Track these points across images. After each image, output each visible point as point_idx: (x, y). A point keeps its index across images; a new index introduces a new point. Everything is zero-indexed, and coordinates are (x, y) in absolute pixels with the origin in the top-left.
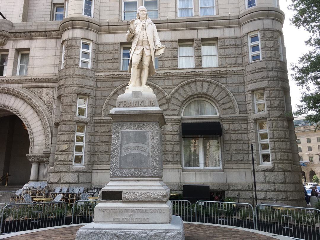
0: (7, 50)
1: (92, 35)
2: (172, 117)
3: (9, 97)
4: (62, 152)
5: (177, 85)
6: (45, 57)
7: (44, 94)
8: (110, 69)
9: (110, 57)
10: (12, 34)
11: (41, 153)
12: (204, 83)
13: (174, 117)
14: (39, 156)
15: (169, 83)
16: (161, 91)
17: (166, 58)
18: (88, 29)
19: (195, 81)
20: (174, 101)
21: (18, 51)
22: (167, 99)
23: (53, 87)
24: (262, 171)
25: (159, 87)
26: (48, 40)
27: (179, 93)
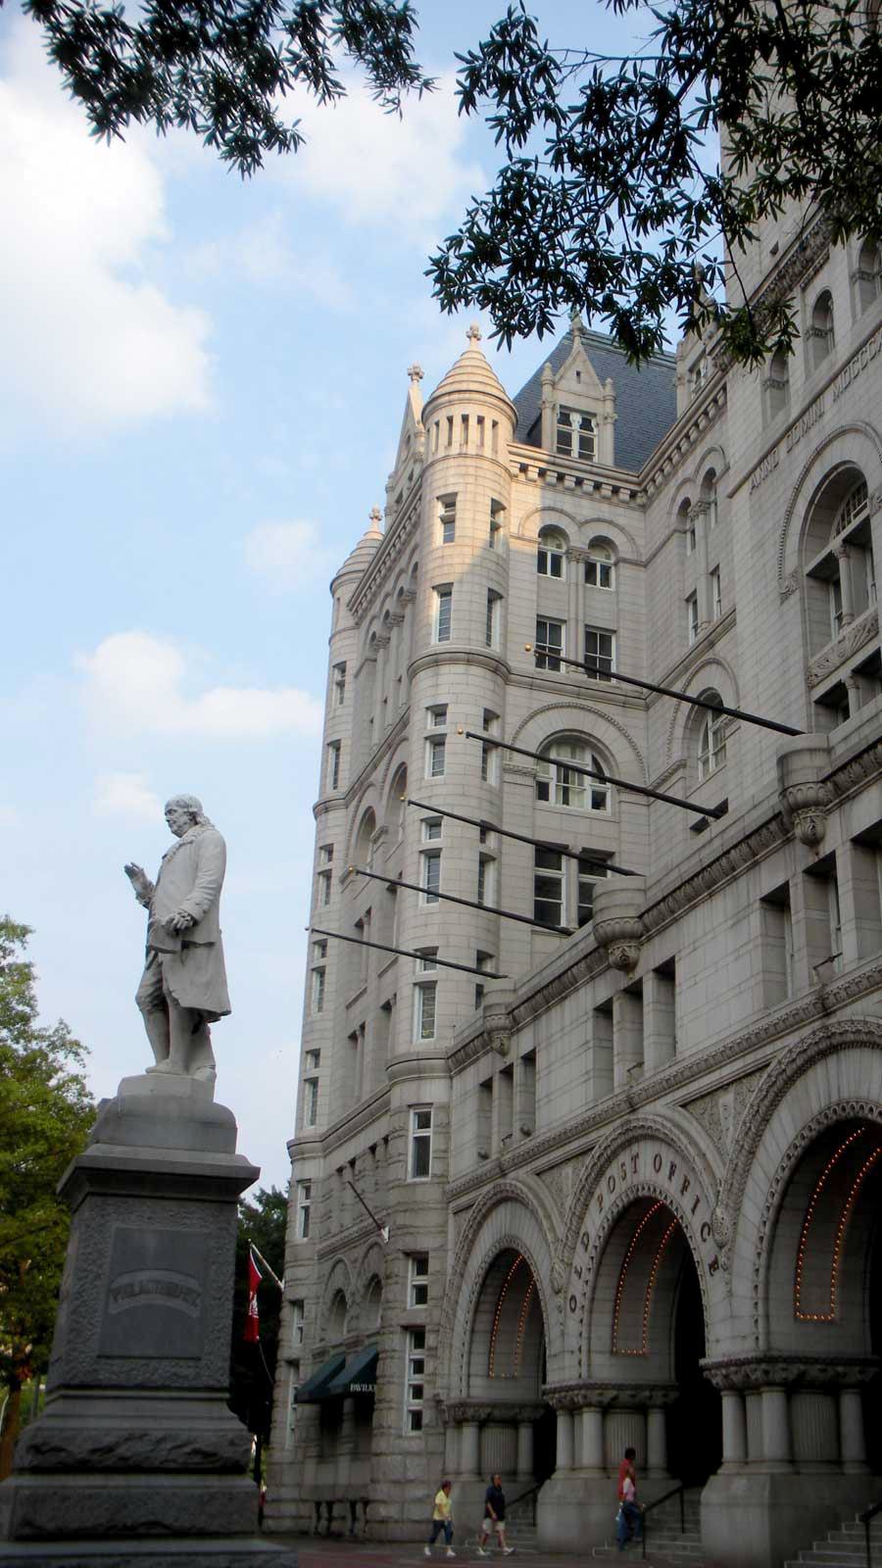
0: (831, 858)
10: (829, 785)
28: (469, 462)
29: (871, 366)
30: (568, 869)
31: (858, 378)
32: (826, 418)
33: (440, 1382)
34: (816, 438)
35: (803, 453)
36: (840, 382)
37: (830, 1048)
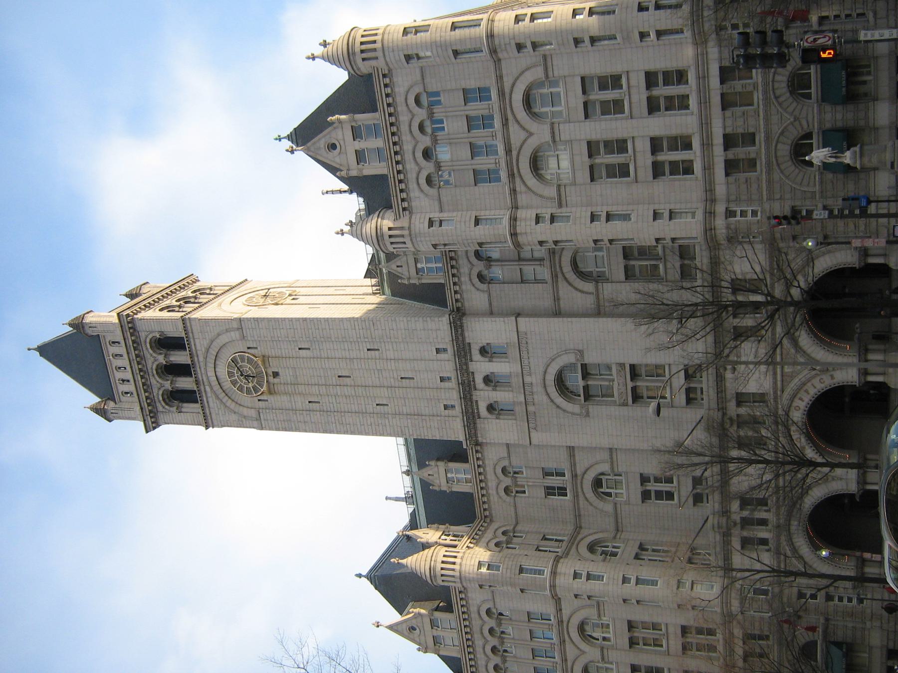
2: (816, 115)
4: (857, 228)
5: (778, 110)
8: (759, 185)
9: (743, 187)
11: (856, 255)
12: (775, 80)
13: (815, 111)
14: (859, 254)
15: (775, 119)
16: (785, 128)
17: (745, 123)
18: (714, 213)
19: (773, 89)
20: (797, 113)
22: (795, 121)
24: (875, 21)
25: (780, 130)
27: (788, 107)
28: (466, 555)
29: (531, 355)
31: (531, 363)
32: (534, 381)
35: (540, 397)
36: (526, 369)
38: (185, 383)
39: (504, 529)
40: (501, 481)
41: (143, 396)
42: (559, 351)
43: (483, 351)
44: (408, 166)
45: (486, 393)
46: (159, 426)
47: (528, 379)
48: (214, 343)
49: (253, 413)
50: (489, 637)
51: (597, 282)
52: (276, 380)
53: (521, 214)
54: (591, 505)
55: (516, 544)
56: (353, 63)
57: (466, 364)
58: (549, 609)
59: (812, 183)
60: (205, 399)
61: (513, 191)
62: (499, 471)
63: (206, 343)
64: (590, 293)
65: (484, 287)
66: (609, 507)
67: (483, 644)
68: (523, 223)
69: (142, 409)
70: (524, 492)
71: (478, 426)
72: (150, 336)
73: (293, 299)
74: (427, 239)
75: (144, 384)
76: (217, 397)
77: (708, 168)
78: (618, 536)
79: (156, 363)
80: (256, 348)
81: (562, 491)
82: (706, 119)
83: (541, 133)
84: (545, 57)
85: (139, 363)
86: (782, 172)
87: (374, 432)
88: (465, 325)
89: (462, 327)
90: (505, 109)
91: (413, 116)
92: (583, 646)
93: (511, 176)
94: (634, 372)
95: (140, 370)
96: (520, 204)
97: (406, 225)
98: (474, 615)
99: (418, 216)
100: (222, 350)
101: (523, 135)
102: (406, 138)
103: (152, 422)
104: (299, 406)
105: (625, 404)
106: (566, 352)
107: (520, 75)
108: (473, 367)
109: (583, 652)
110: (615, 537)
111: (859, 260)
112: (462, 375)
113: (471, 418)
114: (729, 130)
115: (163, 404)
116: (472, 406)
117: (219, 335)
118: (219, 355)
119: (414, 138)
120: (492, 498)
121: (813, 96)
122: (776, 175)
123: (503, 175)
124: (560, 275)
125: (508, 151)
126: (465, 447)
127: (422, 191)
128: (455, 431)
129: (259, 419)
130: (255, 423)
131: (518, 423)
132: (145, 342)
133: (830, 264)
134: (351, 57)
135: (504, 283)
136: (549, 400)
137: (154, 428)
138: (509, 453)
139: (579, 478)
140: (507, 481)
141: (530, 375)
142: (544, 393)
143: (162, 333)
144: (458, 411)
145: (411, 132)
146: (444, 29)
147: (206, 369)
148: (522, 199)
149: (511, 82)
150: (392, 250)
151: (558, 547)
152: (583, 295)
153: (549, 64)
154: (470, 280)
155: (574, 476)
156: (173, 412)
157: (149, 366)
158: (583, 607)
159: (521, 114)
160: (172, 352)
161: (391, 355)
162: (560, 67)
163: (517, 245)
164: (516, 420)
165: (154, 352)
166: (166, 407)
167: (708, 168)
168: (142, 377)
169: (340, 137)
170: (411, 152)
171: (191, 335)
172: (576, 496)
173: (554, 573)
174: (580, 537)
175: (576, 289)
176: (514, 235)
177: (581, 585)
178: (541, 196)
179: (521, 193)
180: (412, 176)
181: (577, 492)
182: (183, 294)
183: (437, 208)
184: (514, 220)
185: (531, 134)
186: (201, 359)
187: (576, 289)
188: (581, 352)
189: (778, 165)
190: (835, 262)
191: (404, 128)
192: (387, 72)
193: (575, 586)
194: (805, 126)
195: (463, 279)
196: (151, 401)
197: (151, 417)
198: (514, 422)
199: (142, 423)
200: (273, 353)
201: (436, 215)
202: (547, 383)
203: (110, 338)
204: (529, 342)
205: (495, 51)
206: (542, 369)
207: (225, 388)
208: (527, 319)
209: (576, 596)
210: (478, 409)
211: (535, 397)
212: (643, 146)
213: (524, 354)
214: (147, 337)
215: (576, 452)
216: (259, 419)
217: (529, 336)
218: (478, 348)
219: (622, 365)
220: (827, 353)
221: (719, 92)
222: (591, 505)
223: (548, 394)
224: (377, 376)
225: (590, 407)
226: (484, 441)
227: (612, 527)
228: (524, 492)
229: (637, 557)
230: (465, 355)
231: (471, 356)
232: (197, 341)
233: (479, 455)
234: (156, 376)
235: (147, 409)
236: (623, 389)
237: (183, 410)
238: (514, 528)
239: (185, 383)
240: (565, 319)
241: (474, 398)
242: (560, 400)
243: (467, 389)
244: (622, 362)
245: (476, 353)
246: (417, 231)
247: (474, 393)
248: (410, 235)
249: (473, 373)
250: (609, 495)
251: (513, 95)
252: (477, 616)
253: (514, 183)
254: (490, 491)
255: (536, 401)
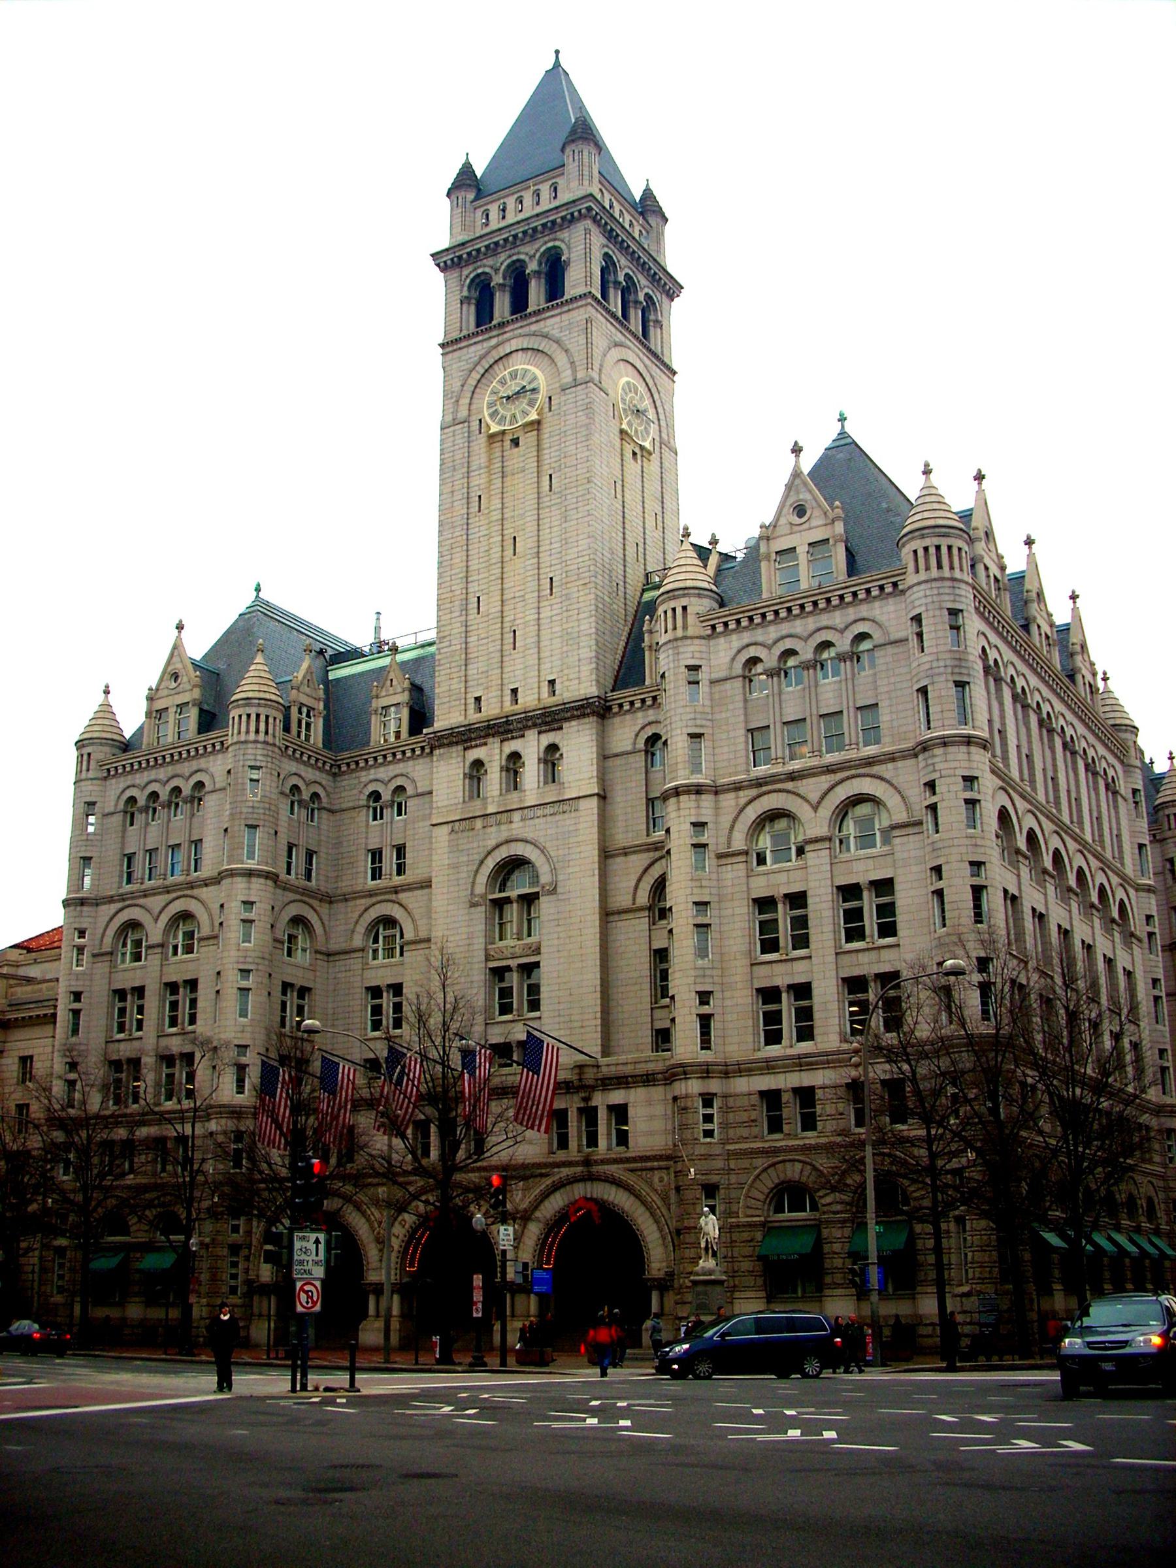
0: (596, 1107)
1: (714, 1086)
3: (607, 1185)
6: (652, 1118)
7: (656, 1180)
9: (744, 1116)
11: (661, 1275)
21: (611, 1108)
23: (667, 1168)
26: (653, 1089)
29: (549, 818)
30: (292, 996)
32: (514, 826)
33: (251, 1272)
34: (504, 833)
35: (494, 835)
37: (591, 1178)
38: (502, 304)
39: (322, 794)
40: (386, 784)
41: (481, 245)
42: (555, 859)
43: (553, 748)
44: (772, 628)
45: (498, 757)
46: (443, 270)
47: (516, 816)
48: (555, 345)
49: (463, 413)
50: (168, 788)
51: (650, 908)
52: (507, 443)
53: (707, 800)
54: (360, 916)
55: (299, 813)
56: (910, 536)
57: (535, 725)
58: (207, 871)
59: (750, 1212)
60: (480, 338)
61: (737, 787)
62: (399, 782)
63: (555, 333)
64: (634, 899)
65: (641, 745)
66: (358, 941)
67: (159, 780)
68: (693, 804)
69: (463, 244)
70: (375, 819)
71: (454, 749)
72: (563, 246)
73: (634, 454)
74: (672, 665)
75: (497, 244)
76: (482, 358)
77: (769, 1066)
78: (318, 956)
79: (527, 259)
80: (550, 410)
81: (376, 874)
82: (811, 1064)
83: (815, 823)
84: (920, 823)
85: (524, 233)
86: (765, 1170)
87: (443, 596)
88: (586, 720)
89: (584, 715)
90: (850, 768)
91: (842, 631)
92: (164, 919)
93: (759, 783)
94: (529, 969)
95: (515, 236)
96: (722, 797)
97: (690, 632)
98: (195, 765)
99: (704, 649)
100: (546, 358)
101: (814, 797)
102: (811, 623)
103: (448, 261)
104: (475, 482)
105: (488, 958)
106: (554, 871)
107: (896, 788)
108: (532, 735)
109: (156, 920)
110: (317, 952)
111: (655, 1279)
112: (519, 721)
113: (465, 737)
114: (819, 1094)
115: (472, 276)
116: (480, 737)
117: (567, 351)
118: (540, 355)
119: (810, 635)
120: (364, 773)
121: (781, 1216)
122: (761, 1162)
123: (762, 770)
124: (658, 854)
125: (792, 777)
126: (425, 731)
127: (739, 651)
128: (446, 717)
129: (455, 422)
130: (449, 418)
131: (460, 806)
132: (555, 240)
133: (649, 1239)
134: (917, 534)
135: (647, 772)
136: (489, 848)
137: (438, 265)
138: (422, 794)
139: (393, 897)
140: (386, 796)
141: (522, 820)
142: (500, 840)
143: (567, 263)
144: (473, 717)
145: (819, 629)
146: (964, 671)
147: (520, 336)
148: (729, 801)
149: (887, 776)
150: (660, 611)
151: (297, 874)
152: (631, 890)
153: (911, 830)
154: (650, 723)
155: (396, 890)
156: (461, 291)
157: (522, 249)
158: (210, 915)
159: (842, 793)
160: (543, 281)
161: (546, 613)
162: (908, 847)
163: (665, 797)
164: (464, 802)
165: (543, 254)
166: (468, 281)
167: (769, 1066)
168: (506, 240)
169: (814, 523)
170: (792, 631)
171: (566, 308)
172: (371, 894)
173: (250, 874)
174: (315, 903)
175: (639, 880)
176: (677, 792)
177: (235, 911)
178: (732, 827)
179: (737, 797)
180: (759, 635)
181: (376, 895)
182: (642, 280)
183: (715, 676)
184: (698, 790)
185: (815, 808)
186: (534, 328)
187: (639, 880)
188: (553, 891)
189: (774, 1165)
190: (650, 1246)
191: (824, 620)
192: (900, 587)
193: (233, 904)
194: (823, 1201)
195: (651, 712)
196: (474, 257)
197: (452, 260)
198: (461, 800)
199: (446, 246)
200: (545, 435)
201: (703, 676)
202: (513, 844)
203: (561, 182)
204: (566, 816)
205: (925, 749)
206: (529, 836)
207: (496, 367)
208: (596, 811)
209: (222, 906)
210: (476, 746)
211: (493, 829)
212: (798, 973)
213: (549, 810)
214: (563, 241)
215: (426, 891)
216: (455, 422)
217: (573, 815)
218: (557, 742)
219: (537, 951)
220: (535, 1238)
221: (781, 1086)
222: (360, 916)
223: (498, 846)
224: (517, 594)
225: (483, 908)
226: (435, 758)
227: (334, 946)
228: (375, 819)
229: (286, 987)
230: (546, 723)
231: (545, 731)
232: (557, 319)
233: (418, 752)
234: (509, 261)
235: (463, 252)
236: (507, 953)
237: (465, 307)
238: (324, 808)
239: (502, 304)
240: (596, 866)
241: (490, 740)
242: (490, 864)
243: (501, 730)
244: (543, 950)
245: (547, 739)
246: (681, 650)
247: (497, 740)
248: (676, 639)
249: (523, 736)
250: (376, 941)
251: (868, 779)
252: (195, 768)
253: (750, 787)
254: (372, 771)
255: (489, 830)
